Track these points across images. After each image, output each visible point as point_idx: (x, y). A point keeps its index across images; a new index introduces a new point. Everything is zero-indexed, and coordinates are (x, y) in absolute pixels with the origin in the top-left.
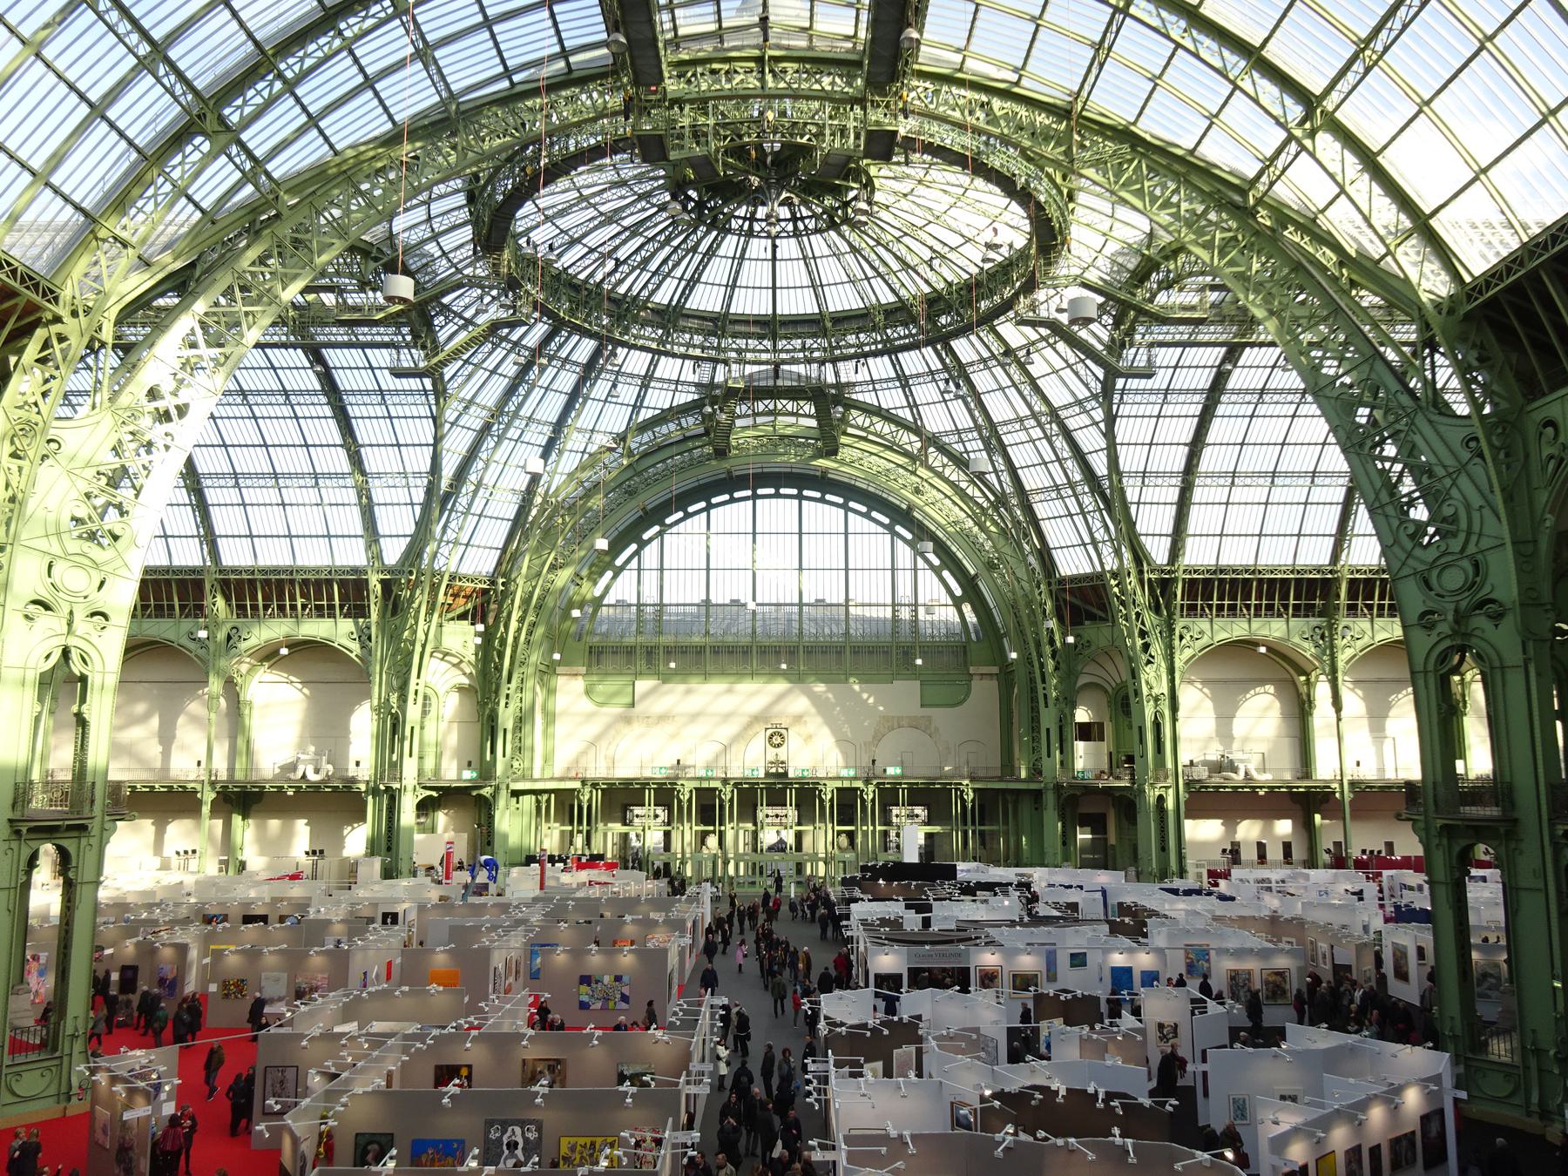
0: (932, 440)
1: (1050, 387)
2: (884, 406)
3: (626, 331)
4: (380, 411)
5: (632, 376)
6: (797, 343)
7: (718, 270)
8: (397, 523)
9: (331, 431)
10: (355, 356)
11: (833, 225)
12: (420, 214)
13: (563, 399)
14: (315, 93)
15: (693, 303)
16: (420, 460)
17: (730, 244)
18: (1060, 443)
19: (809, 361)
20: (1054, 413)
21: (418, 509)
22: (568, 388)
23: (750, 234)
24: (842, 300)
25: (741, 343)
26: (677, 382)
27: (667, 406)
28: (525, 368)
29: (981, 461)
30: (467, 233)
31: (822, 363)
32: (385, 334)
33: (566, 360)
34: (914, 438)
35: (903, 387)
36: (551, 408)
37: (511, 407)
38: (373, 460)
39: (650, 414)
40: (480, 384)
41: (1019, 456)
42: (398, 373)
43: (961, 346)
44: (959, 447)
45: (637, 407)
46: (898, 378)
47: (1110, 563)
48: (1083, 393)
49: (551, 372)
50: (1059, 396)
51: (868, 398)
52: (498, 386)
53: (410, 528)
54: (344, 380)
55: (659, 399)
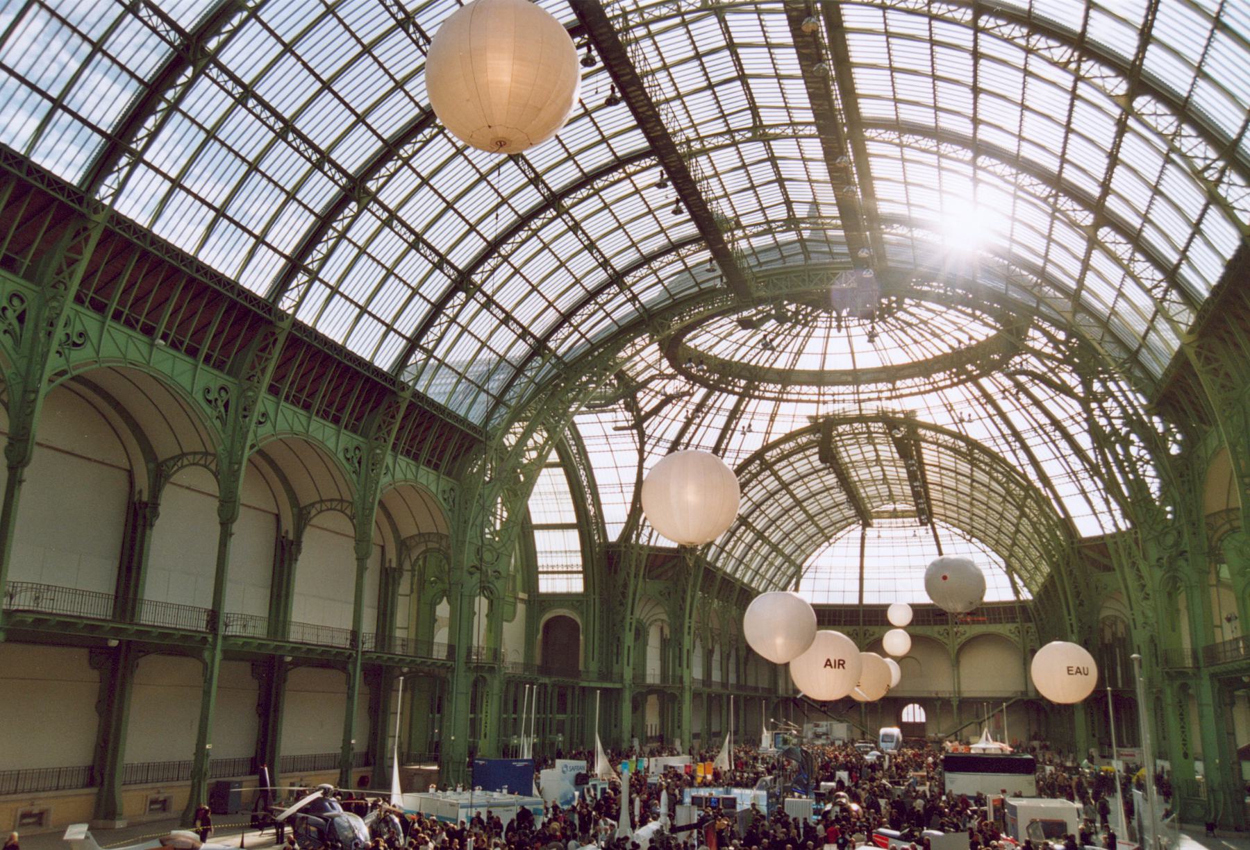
0: (973, 444)
1: (1049, 405)
3: (757, 388)
5: (763, 414)
7: (815, 345)
13: (718, 432)
17: (820, 332)
18: (1063, 445)
19: (879, 399)
20: (1056, 423)
22: (722, 425)
23: (830, 327)
24: (899, 358)
25: (835, 389)
27: (788, 431)
29: (1011, 459)
30: (655, 346)
40: (666, 426)
41: (1041, 452)
42: (616, 429)
43: (984, 381)
44: (996, 449)
45: (768, 433)
47: (1110, 529)
48: (1072, 413)
49: (709, 417)
50: (1059, 415)
52: (677, 427)
53: (625, 519)
55: (781, 428)
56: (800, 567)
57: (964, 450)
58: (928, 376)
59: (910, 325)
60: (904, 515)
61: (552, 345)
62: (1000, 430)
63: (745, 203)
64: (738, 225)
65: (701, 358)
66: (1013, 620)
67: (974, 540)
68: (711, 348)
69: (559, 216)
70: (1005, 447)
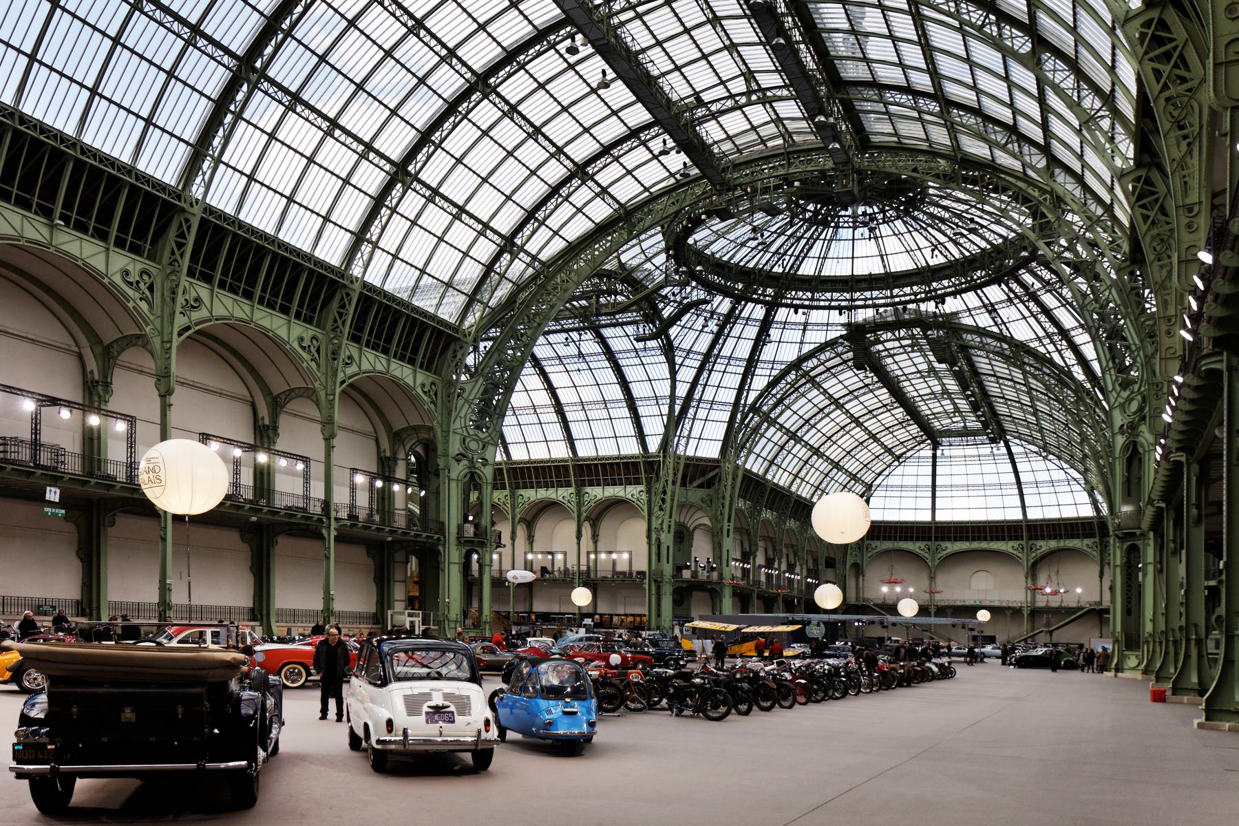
2: (981, 325)
4: (637, 361)
6: (907, 290)
8: (654, 428)
9: (609, 375)
10: (618, 331)
11: (907, 213)
12: (637, 250)
14: (554, 222)
15: (825, 273)
16: (664, 389)
19: (916, 301)
21: (665, 418)
26: (828, 325)
28: (722, 328)
31: (923, 300)
32: (629, 316)
33: (748, 319)
34: (1006, 346)
35: (990, 312)
36: (744, 350)
37: (716, 352)
38: (638, 390)
39: (812, 347)
44: (1042, 350)
46: (985, 306)
51: (968, 321)
53: (662, 430)
54: (615, 345)
55: (816, 337)
56: (871, 485)
57: (1007, 353)
58: (964, 275)
59: (943, 220)
60: (974, 433)
61: (518, 241)
62: (1044, 329)
63: (701, 77)
64: (700, 103)
65: (700, 255)
66: (1092, 536)
67: (1051, 457)
68: (732, 258)
69: (485, 96)
70: (1051, 348)
